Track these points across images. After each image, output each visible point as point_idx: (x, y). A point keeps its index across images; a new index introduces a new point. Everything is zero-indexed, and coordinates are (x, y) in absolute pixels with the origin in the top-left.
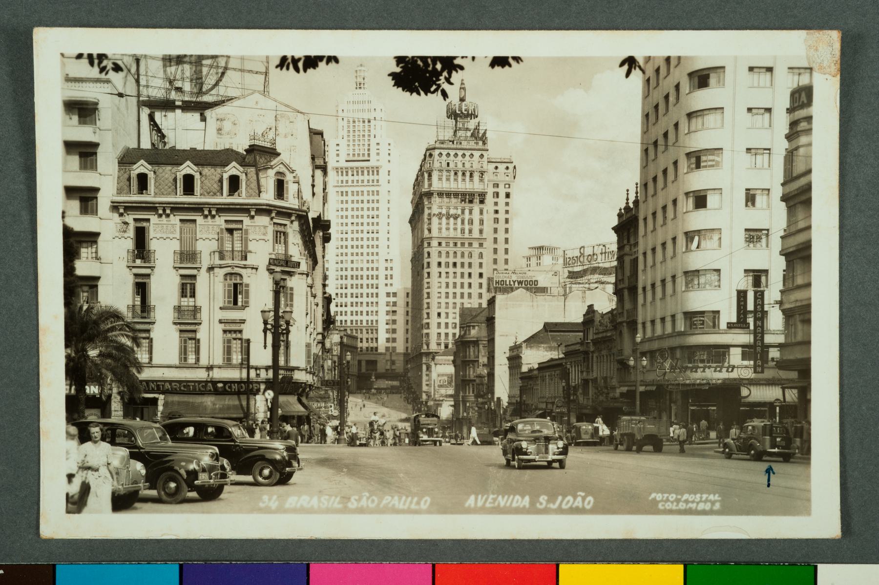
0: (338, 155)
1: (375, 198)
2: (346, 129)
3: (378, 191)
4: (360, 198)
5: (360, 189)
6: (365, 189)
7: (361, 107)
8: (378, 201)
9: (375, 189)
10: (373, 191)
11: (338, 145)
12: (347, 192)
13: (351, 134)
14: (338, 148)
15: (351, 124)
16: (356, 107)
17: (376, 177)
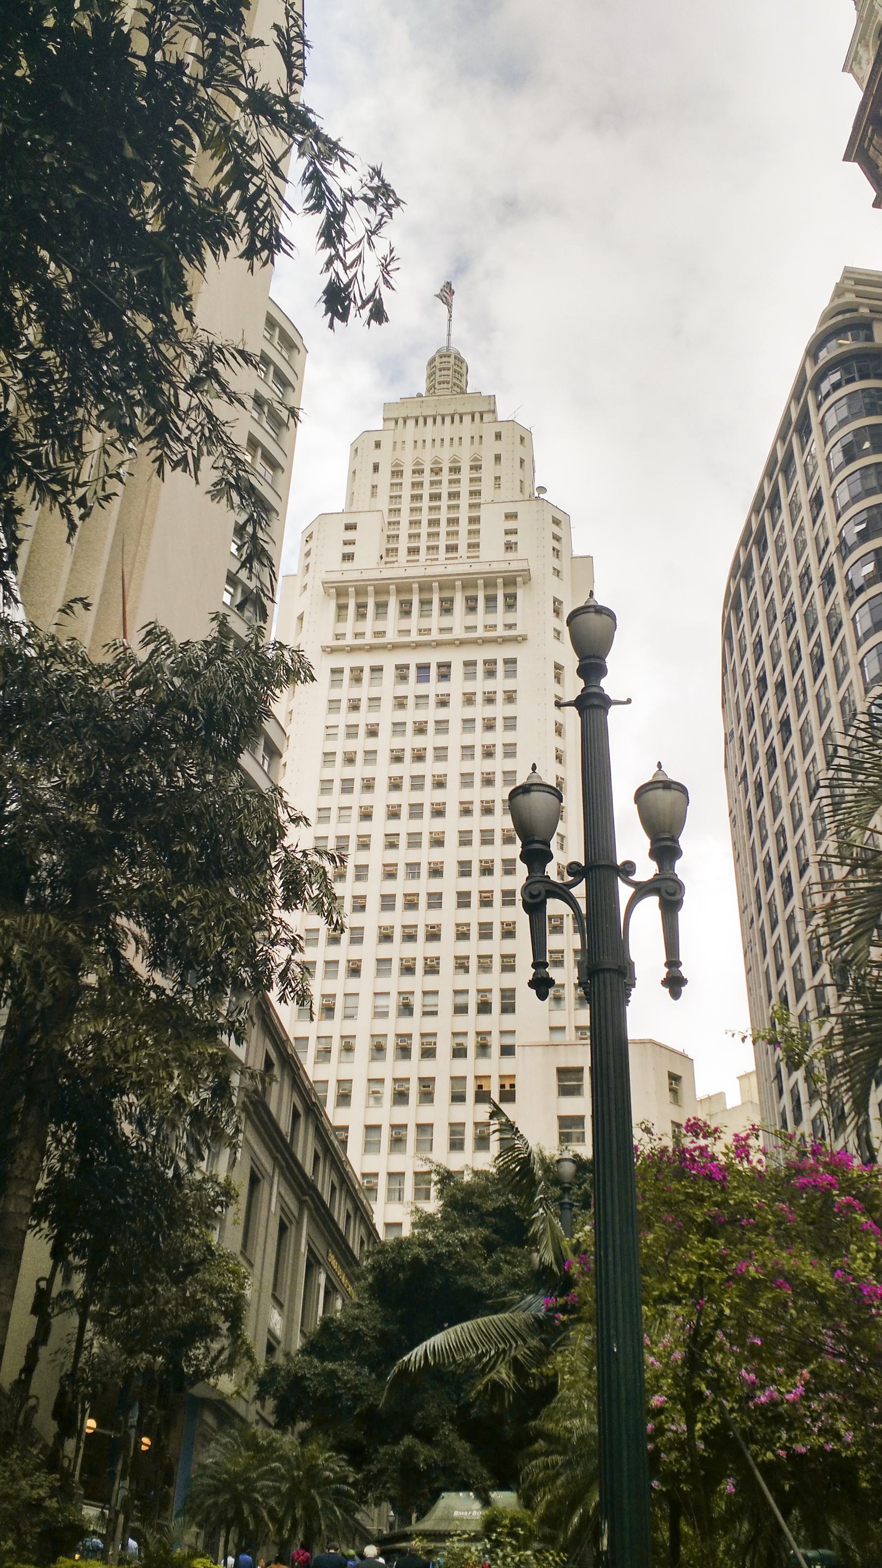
0: (348, 557)
1: (500, 684)
2: (384, 491)
3: (511, 662)
4: (433, 687)
5: (433, 658)
6: (456, 658)
7: (447, 430)
8: (510, 697)
9: (499, 654)
10: (490, 663)
11: (350, 527)
12: (377, 669)
13: (406, 504)
14: (350, 535)
15: (408, 479)
16: (429, 431)
17: (500, 617)
